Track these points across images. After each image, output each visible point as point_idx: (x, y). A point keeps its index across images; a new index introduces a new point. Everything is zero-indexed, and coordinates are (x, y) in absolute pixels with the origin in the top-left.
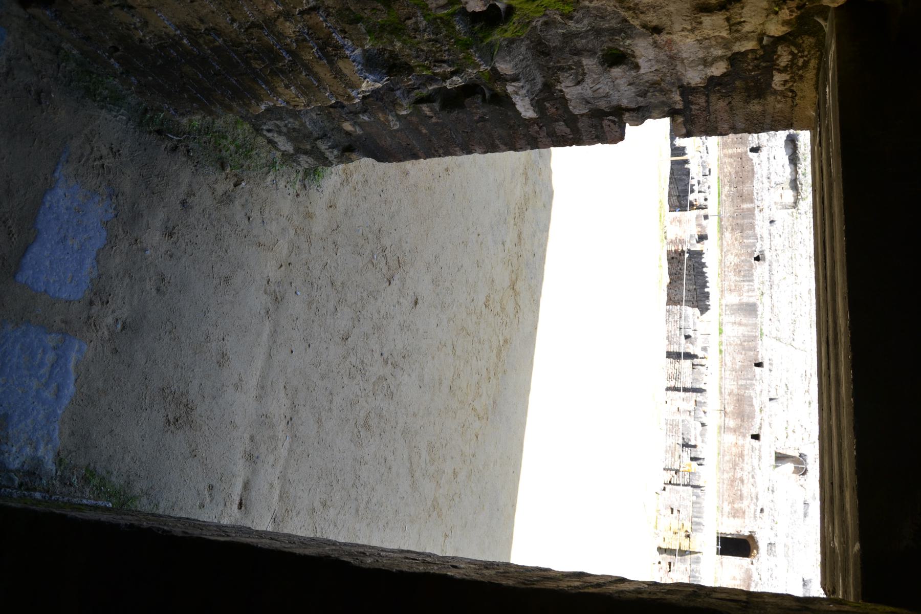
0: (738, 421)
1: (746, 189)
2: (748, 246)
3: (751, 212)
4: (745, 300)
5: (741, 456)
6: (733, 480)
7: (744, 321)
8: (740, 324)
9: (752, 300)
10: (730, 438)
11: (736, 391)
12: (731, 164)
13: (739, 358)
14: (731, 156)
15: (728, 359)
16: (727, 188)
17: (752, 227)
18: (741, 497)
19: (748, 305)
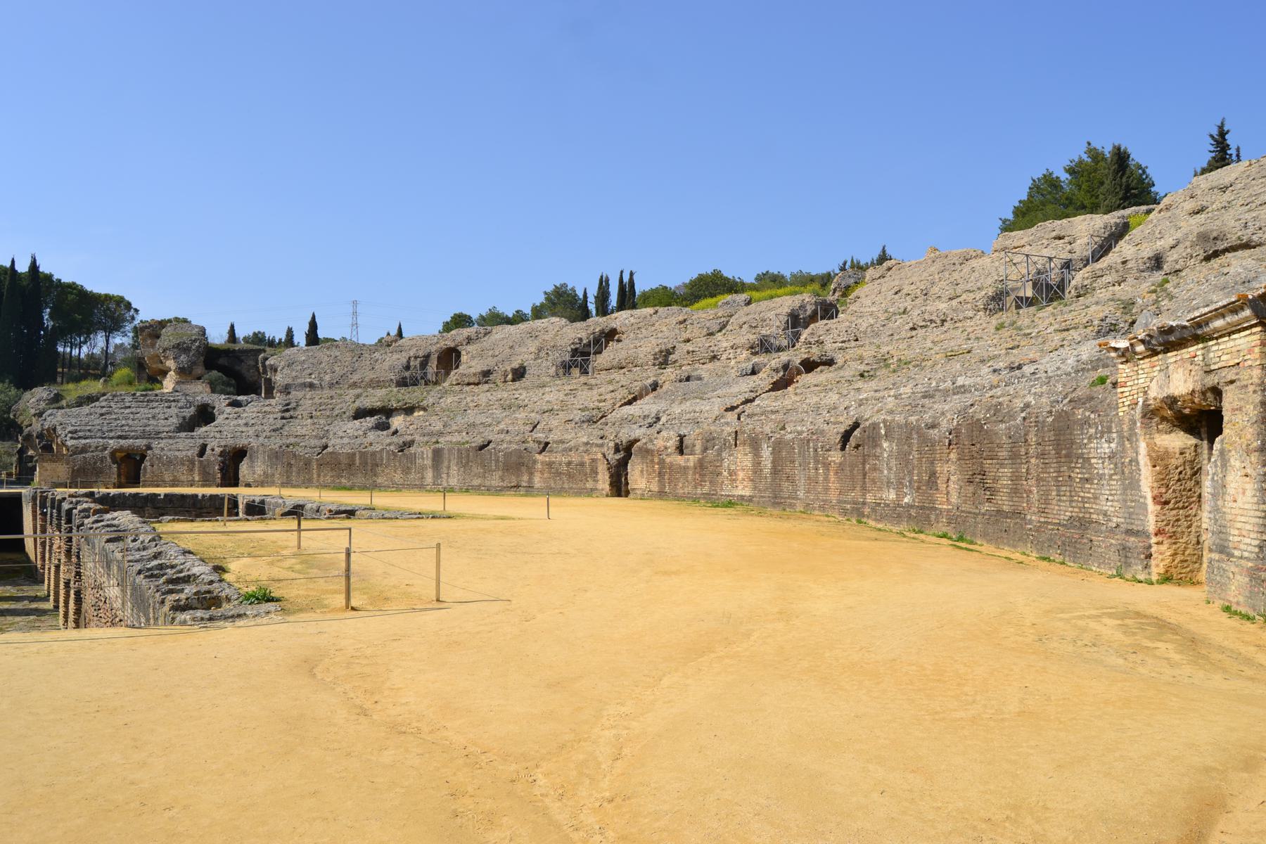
0: (524, 469)
1: (345, 461)
2: (388, 459)
3: (363, 454)
4: (428, 462)
5: (550, 464)
6: (570, 476)
7: (446, 463)
8: (449, 468)
9: (430, 455)
10: (537, 481)
11: (500, 473)
12: (325, 476)
13: (475, 470)
14: (319, 476)
15: (476, 482)
16: (343, 480)
17: (374, 454)
18: (582, 464)
19: (434, 460)
